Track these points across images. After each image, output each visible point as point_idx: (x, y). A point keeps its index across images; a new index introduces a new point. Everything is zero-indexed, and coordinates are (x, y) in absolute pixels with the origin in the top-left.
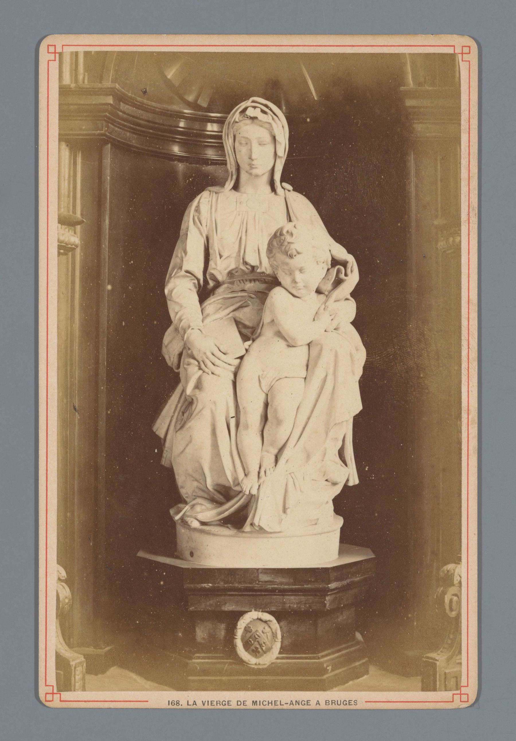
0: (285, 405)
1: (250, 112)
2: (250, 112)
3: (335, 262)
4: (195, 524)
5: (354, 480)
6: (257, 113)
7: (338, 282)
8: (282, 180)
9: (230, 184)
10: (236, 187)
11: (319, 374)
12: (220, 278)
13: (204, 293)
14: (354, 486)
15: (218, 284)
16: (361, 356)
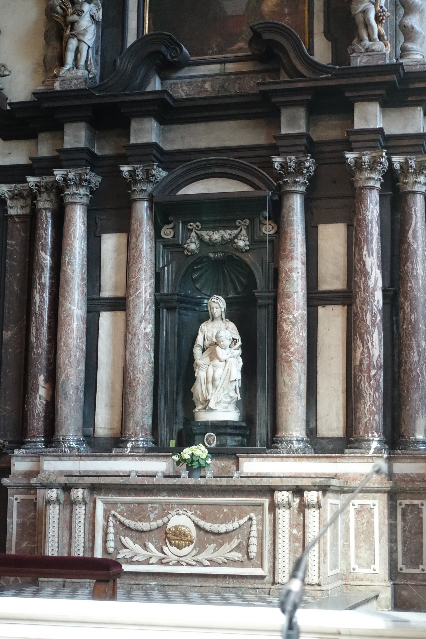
0: (217, 376)
1: (213, 300)
2: (213, 300)
3: (234, 339)
4: (197, 410)
5: (240, 398)
6: (215, 300)
7: (235, 344)
8: (226, 318)
9: (210, 320)
10: (213, 320)
11: (227, 368)
12: (207, 346)
13: (204, 351)
14: (240, 400)
15: (207, 348)
16: (241, 364)
